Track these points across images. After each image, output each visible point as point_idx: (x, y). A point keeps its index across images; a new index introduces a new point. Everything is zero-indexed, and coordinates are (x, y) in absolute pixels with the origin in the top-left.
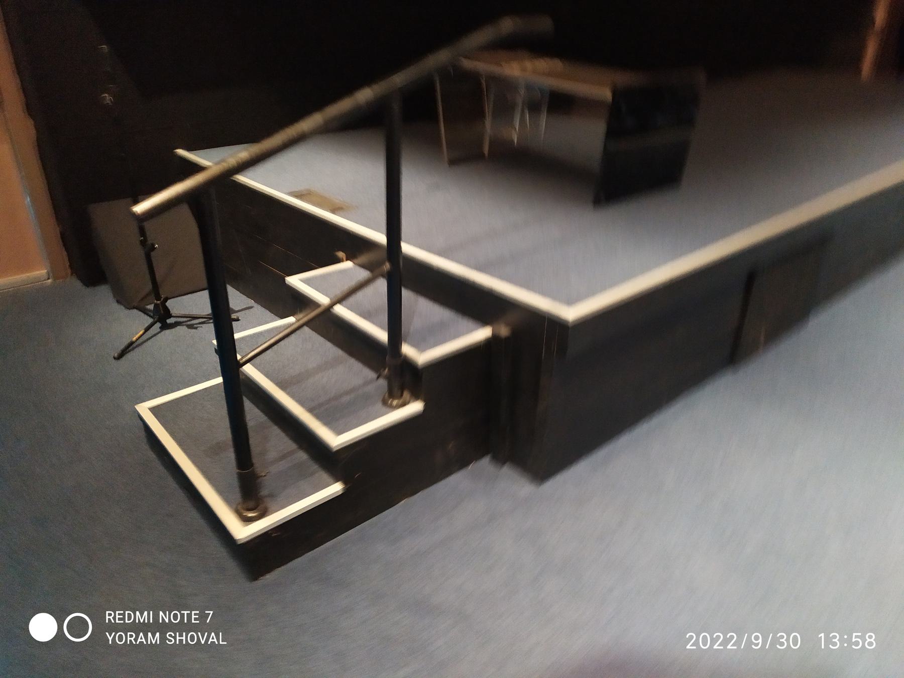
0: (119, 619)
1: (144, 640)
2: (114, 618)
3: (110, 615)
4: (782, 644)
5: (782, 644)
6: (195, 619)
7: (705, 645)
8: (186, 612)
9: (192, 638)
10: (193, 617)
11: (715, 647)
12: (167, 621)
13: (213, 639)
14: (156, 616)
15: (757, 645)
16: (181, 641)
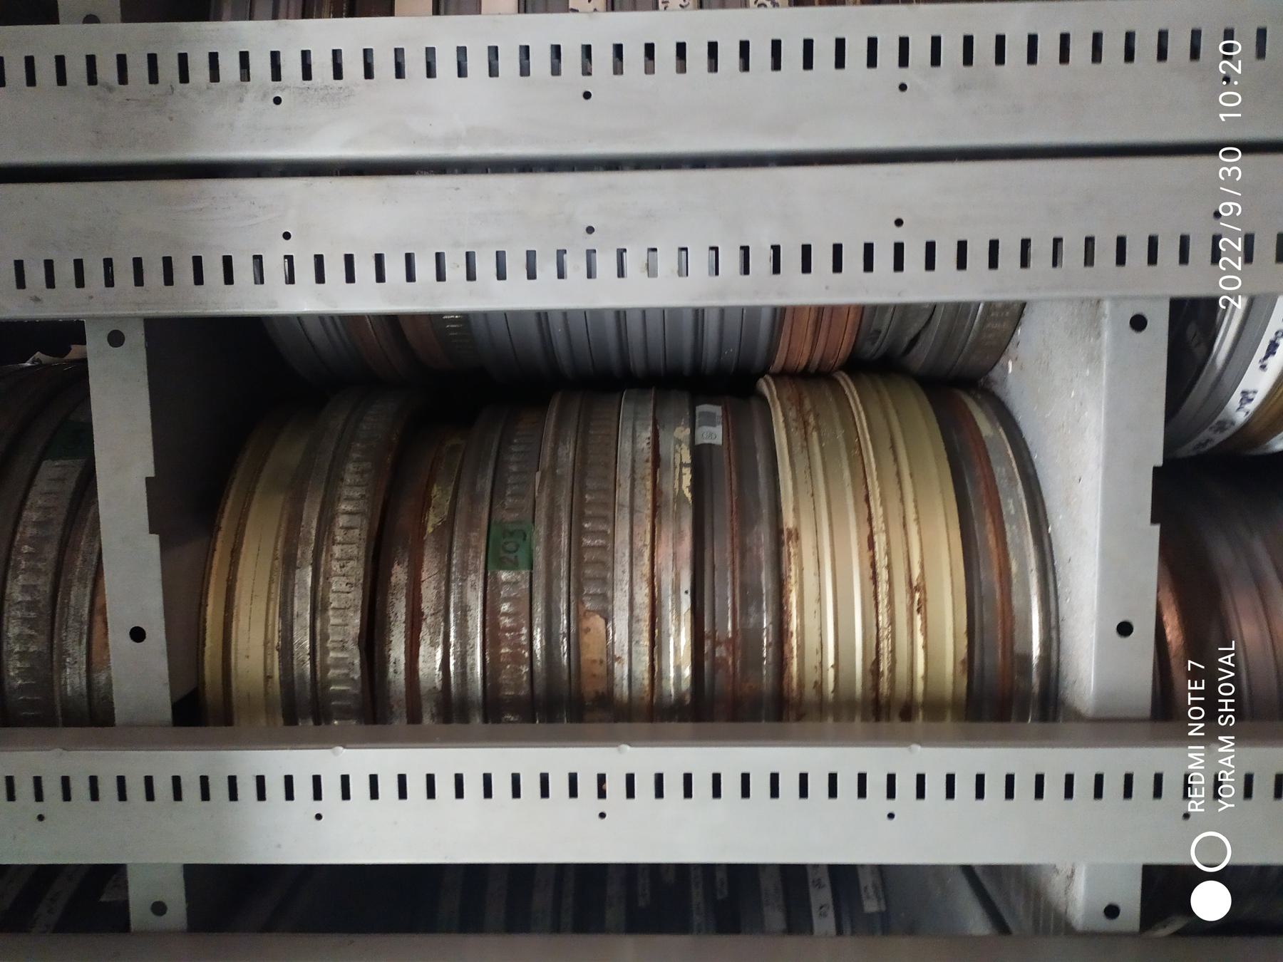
0: (1199, 792)
1: (1229, 758)
2: (1198, 800)
3: (1193, 806)
4: (1235, 173)
5: (1235, 173)
6: (1200, 685)
7: (1235, 283)
8: (1190, 699)
9: (1227, 689)
10: (1196, 688)
11: (1239, 268)
12: (1202, 725)
13: (1226, 660)
14: (1195, 741)
15: (1236, 209)
16: (1230, 705)
